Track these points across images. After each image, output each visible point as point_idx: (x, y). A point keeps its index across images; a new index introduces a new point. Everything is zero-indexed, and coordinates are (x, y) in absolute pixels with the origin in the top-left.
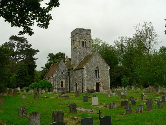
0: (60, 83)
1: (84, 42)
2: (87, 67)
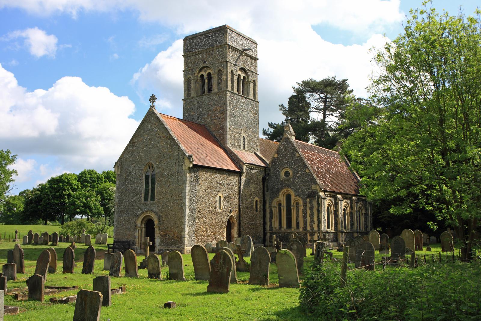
1: (205, 76)
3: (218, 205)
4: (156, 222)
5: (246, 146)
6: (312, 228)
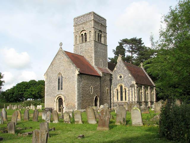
1: (84, 35)
3: (91, 91)
4: (63, 99)
5: (102, 65)
6: (132, 100)
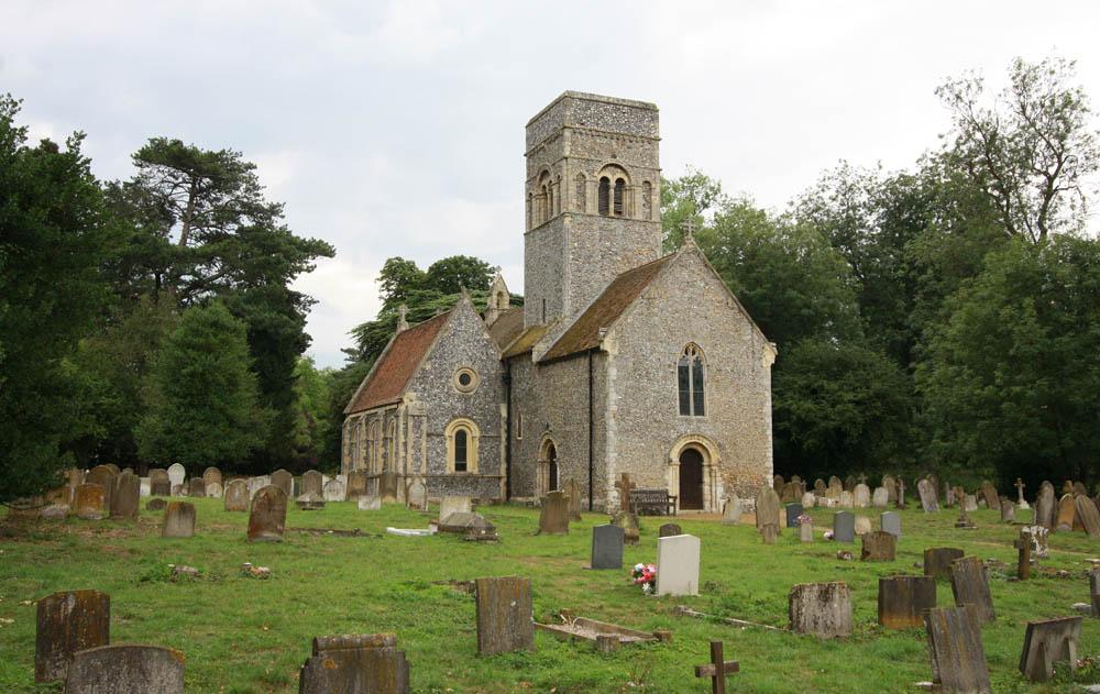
0: (451, 446)
1: (613, 183)
2: (621, 339)
4: (713, 456)
